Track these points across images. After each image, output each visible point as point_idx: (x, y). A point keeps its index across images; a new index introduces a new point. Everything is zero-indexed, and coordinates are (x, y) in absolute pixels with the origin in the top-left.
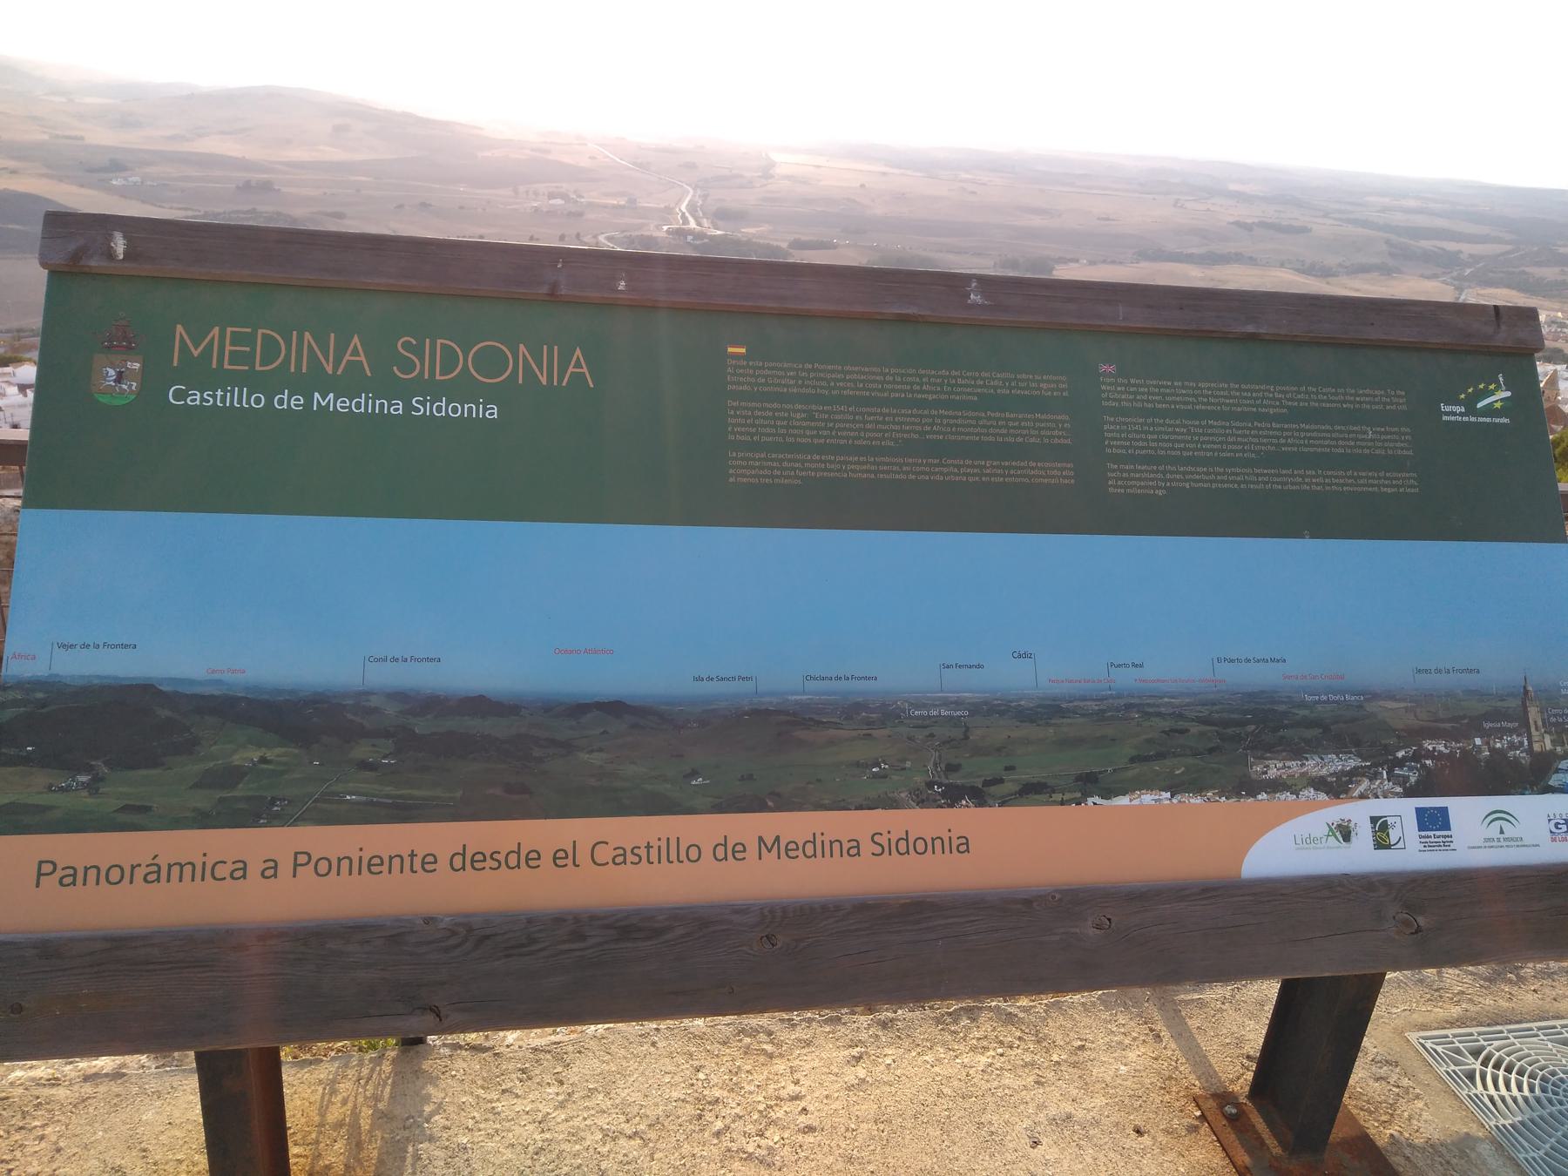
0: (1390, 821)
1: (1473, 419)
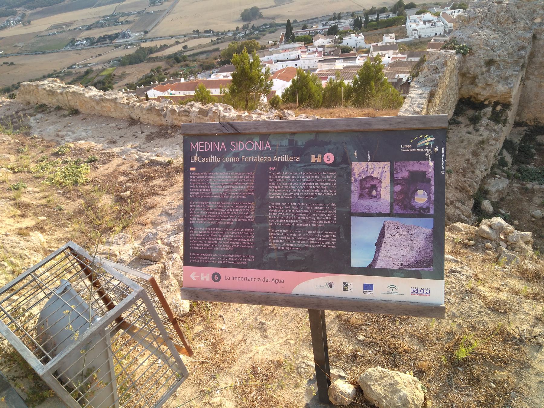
1: (414, 150)
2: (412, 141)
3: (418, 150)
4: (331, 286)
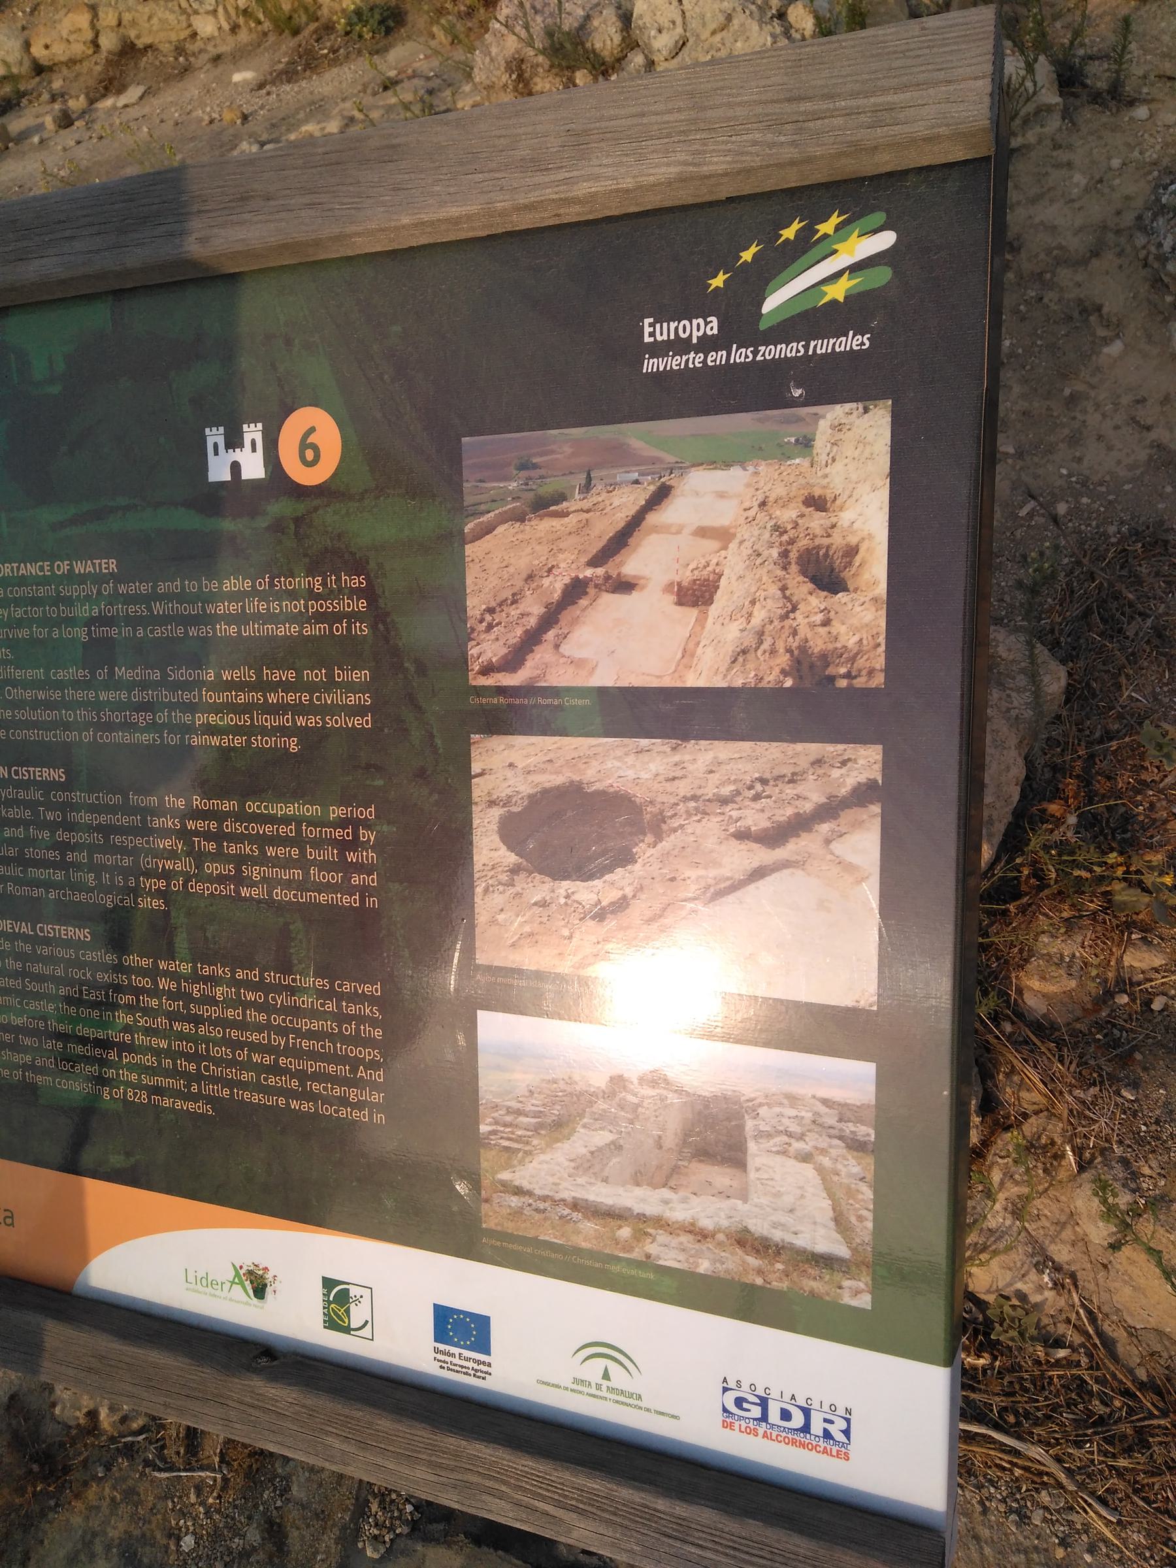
0: (354, 1291)
1: (741, 355)
2: (718, 281)
3: (768, 352)
4: (260, 1291)
